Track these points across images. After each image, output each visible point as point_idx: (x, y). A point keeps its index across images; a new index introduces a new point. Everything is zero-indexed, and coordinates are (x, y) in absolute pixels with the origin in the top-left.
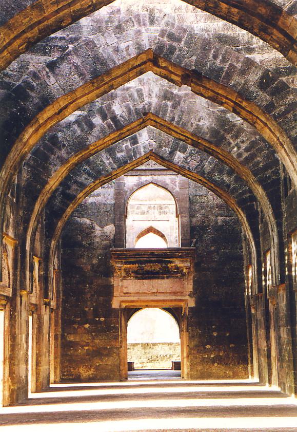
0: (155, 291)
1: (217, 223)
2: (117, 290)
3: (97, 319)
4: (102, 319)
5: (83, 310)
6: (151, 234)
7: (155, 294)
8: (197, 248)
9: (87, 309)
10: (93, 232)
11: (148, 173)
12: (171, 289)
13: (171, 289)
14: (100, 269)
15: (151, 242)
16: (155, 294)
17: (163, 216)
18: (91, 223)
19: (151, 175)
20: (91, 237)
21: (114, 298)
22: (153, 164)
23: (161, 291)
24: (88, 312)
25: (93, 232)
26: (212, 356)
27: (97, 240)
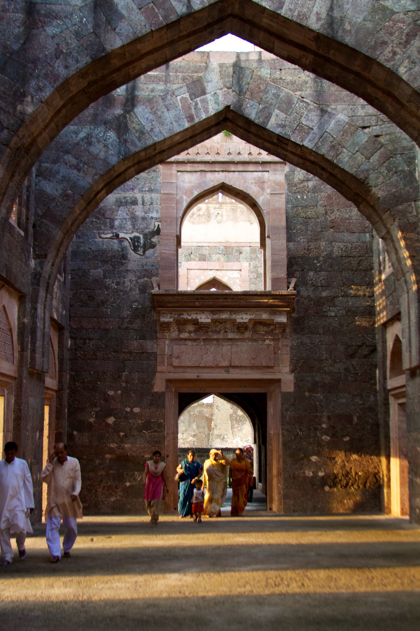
0: (226, 363)
1: (332, 252)
2: (163, 362)
3: (128, 409)
4: (136, 410)
5: (105, 393)
7: (227, 368)
8: (298, 292)
9: (111, 393)
10: (122, 264)
11: (217, 168)
12: (253, 362)
13: (253, 362)
14: (134, 325)
16: (227, 368)
17: (230, 265)
18: (120, 250)
19: (223, 171)
20: (119, 272)
21: (158, 375)
23: (237, 364)
24: (112, 397)
25: (122, 264)
26: (321, 474)
27: (131, 277)
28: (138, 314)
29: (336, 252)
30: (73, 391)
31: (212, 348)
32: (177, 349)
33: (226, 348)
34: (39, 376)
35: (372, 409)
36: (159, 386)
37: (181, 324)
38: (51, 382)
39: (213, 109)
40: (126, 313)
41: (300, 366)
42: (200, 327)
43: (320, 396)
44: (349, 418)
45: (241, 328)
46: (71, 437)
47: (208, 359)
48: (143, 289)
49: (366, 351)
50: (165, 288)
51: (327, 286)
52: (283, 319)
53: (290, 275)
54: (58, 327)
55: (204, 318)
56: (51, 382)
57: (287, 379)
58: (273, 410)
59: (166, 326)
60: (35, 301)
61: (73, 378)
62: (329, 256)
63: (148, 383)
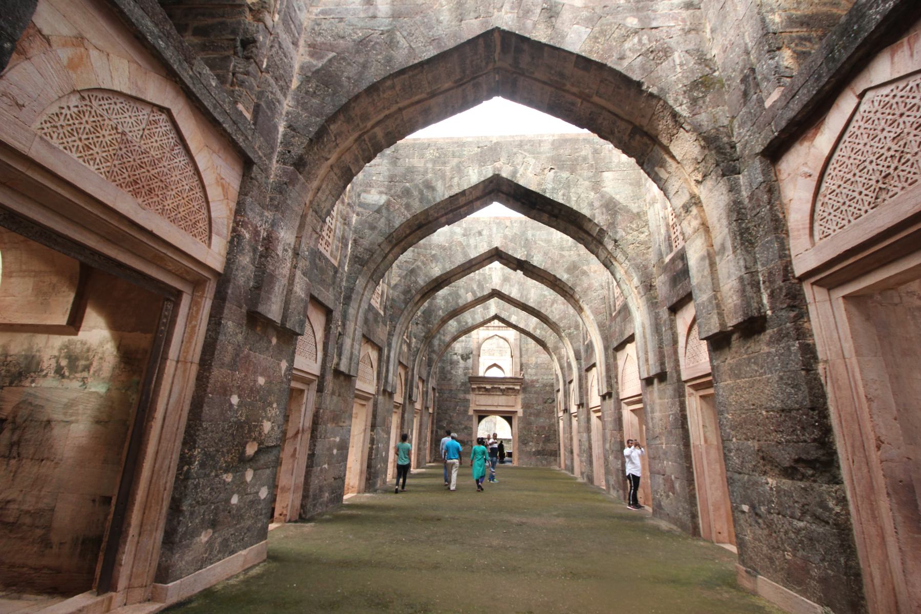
6: (495, 368)
7: (497, 406)
15: (494, 373)
16: (497, 406)
22: (496, 322)
28: (463, 384)
29: (539, 362)
30: (438, 414)
31: (491, 398)
32: (478, 397)
33: (496, 398)
34: (427, 408)
35: (553, 425)
36: (471, 413)
37: (479, 388)
38: (431, 411)
39: (492, 314)
40: (459, 384)
41: (526, 406)
42: (486, 390)
43: (533, 418)
44: (544, 428)
45: (501, 390)
46: (437, 432)
47: (489, 403)
48: (465, 374)
49: (550, 401)
50: (475, 375)
51: (536, 375)
52: (518, 387)
53: (521, 370)
54: (434, 389)
55: (488, 387)
56: (431, 411)
57: (520, 412)
58: (515, 422)
59: (473, 389)
60: (428, 381)
61: (438, 409)
62: (536, 363)
63: (466, 411)
